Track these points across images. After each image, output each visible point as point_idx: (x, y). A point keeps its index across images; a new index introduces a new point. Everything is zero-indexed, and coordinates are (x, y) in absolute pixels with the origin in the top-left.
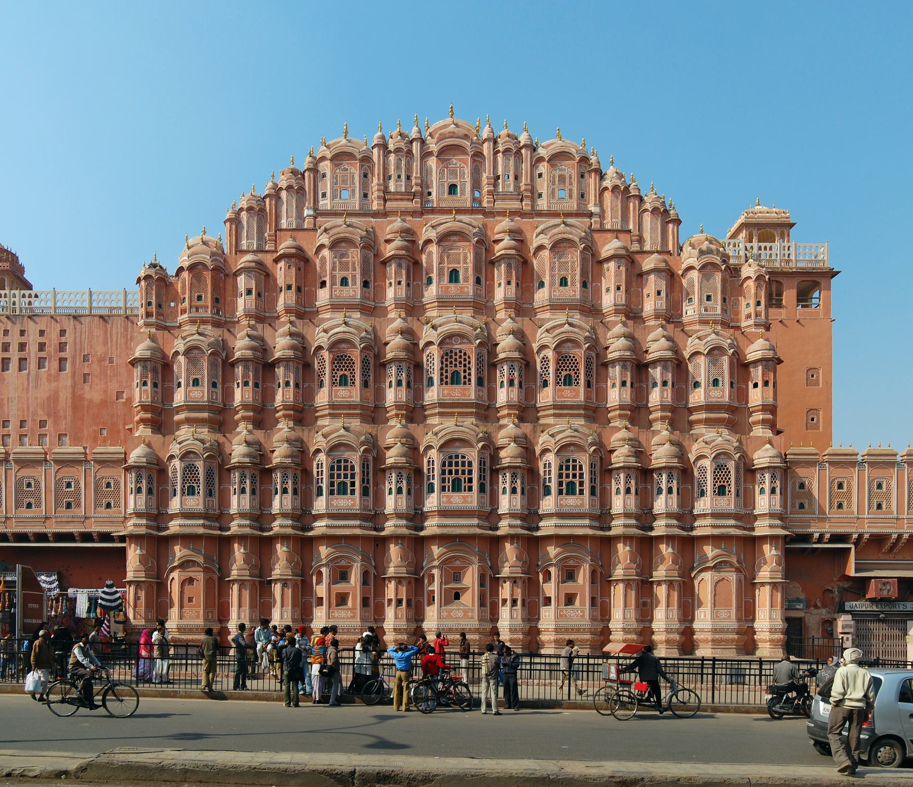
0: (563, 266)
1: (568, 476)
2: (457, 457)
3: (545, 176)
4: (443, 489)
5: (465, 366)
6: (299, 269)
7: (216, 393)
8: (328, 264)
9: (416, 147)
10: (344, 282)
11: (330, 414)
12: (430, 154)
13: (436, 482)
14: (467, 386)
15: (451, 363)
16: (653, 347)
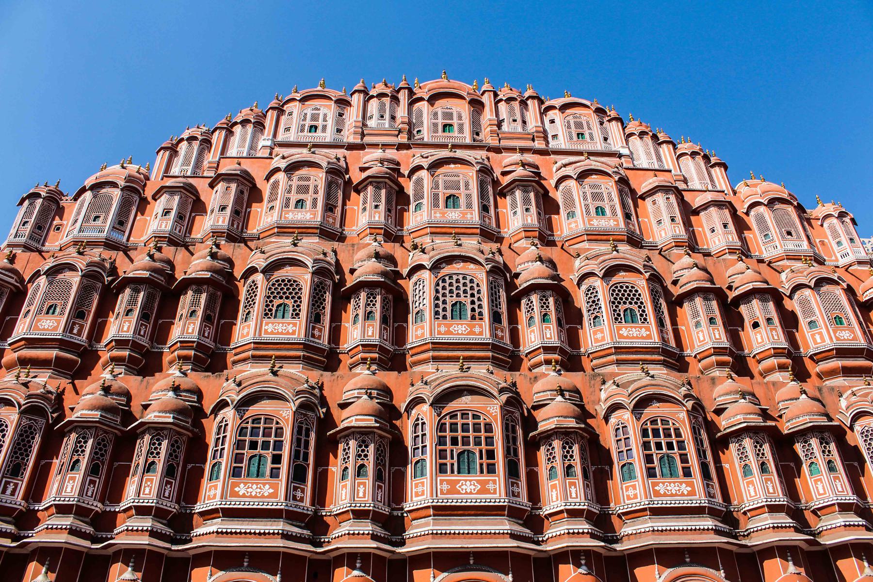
0: (597, 196)
1: (659, 446)
2: (464, 415)
3: (557, 121)
4: (442, 469)
5: (472, 295)
6: (242, 192)
7: (82, 327)
8: (280, 187)
9: (403, 96)
10: (300, 203)
11: (253, 357)
12: (421, 99)
13: (430, 459)
14: (477, 322)
15: (451, 292)
16: (737, 280)
